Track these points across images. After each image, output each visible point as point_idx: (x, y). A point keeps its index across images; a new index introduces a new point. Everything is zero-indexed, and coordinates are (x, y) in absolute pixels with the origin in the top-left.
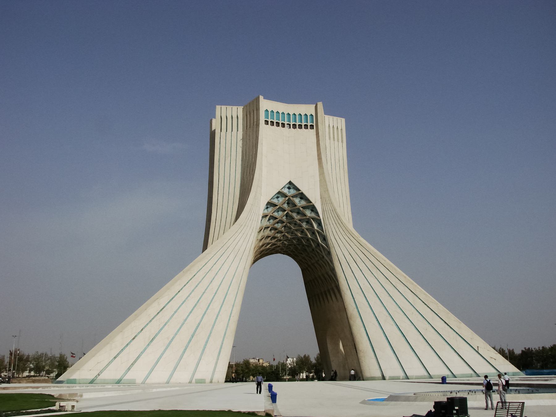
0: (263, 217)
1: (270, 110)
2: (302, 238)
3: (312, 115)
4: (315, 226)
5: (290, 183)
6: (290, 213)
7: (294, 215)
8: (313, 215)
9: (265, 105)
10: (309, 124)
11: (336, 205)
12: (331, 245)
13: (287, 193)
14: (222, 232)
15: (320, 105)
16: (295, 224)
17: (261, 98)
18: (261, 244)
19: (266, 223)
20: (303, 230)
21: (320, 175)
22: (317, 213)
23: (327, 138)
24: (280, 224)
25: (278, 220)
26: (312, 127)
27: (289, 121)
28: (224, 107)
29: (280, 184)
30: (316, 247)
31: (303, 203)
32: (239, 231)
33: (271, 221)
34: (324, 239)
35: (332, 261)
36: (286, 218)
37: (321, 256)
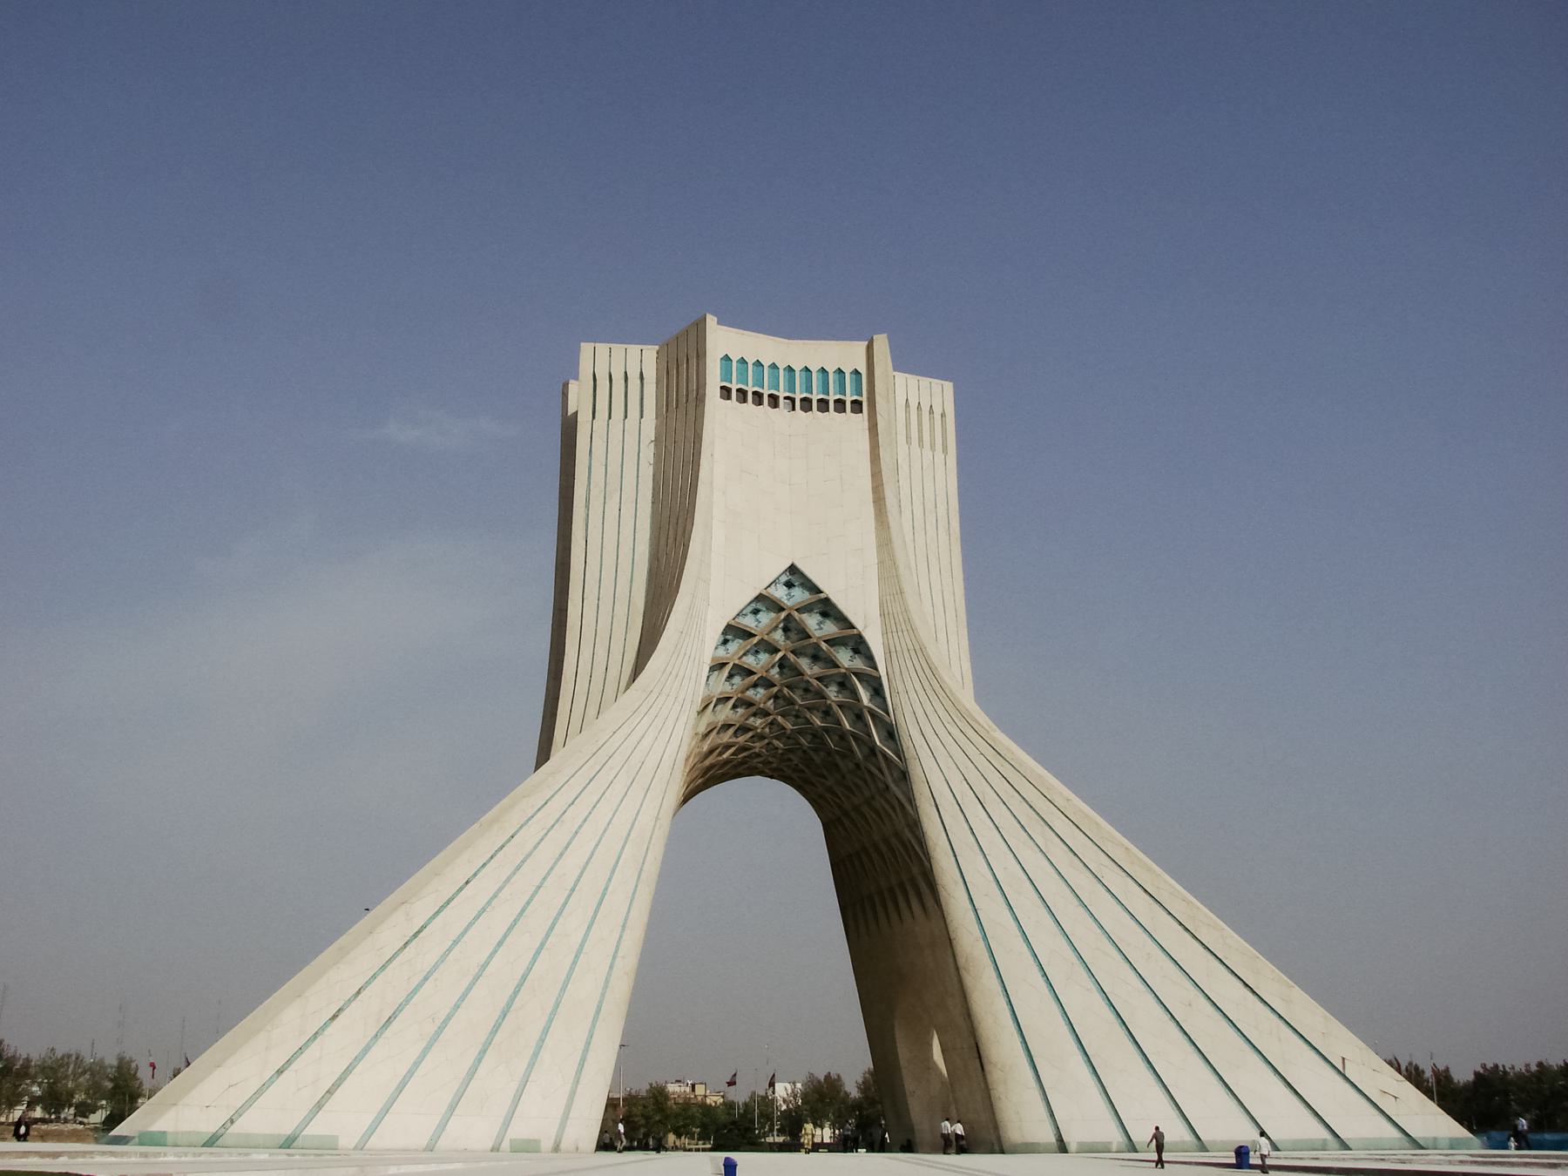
0: (712, 669)
1: (735, 359)
2: (826, 730)
3: (856, 372)
4: (865, 696)
5: (793, 569)
6: (791, 657)
7: (804, 663)
8: (858, 663)
9: (723, 341)
10: (849, 399)
11: (924, 635)
12: (909, 753)
13: (785, 600)
14: (592, 711)
15: (881, 343)
16: (806, 690)
17: (711, 321)
18: (705, 748)
19: (720, 685)
20: (830, 707)
21: (880, 547)
22: (870, 659)
23: (902, 438)
24: (761, 691)
25: (756, 677)
26: (857, 406)
27: (792, 388)
28: (602, 348)
29: (764, 573)
30: (866, 758)
31: (830, 628)
32: (644, 709)
33: (737, 680)
34: (891, 734)
35: (911, 800)
36: (781, 673)
37: (881, 786)
